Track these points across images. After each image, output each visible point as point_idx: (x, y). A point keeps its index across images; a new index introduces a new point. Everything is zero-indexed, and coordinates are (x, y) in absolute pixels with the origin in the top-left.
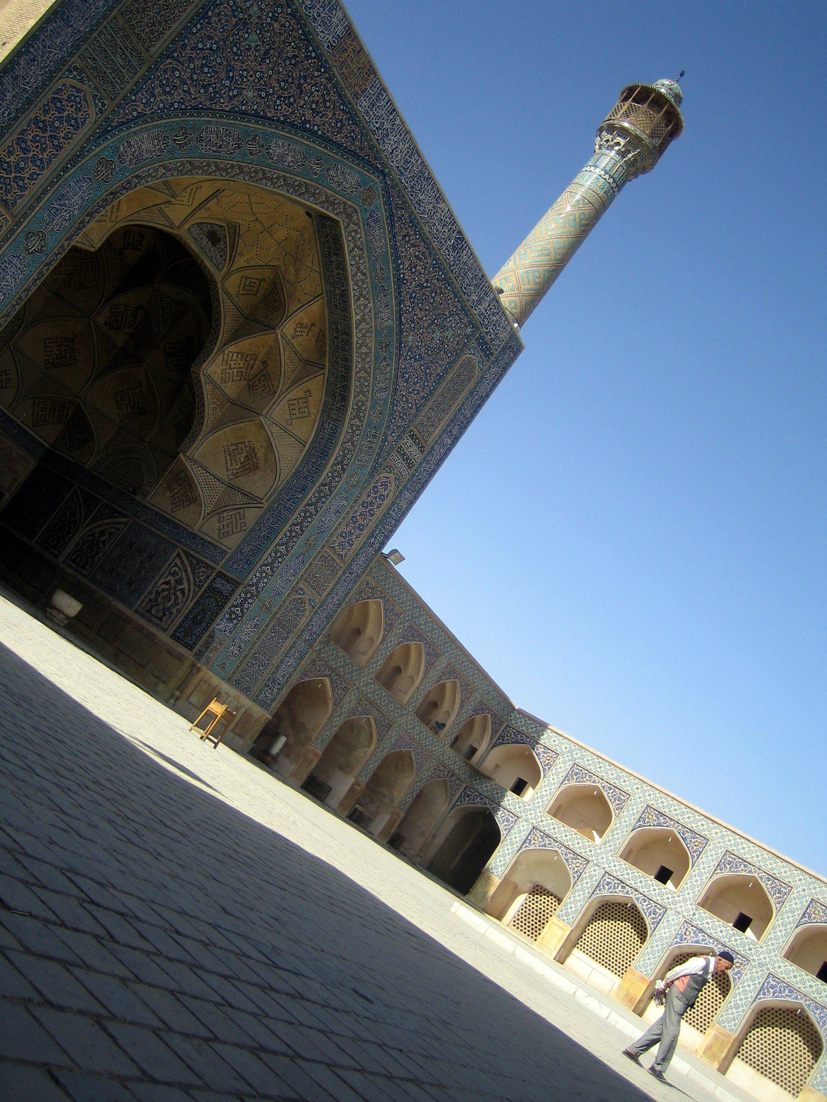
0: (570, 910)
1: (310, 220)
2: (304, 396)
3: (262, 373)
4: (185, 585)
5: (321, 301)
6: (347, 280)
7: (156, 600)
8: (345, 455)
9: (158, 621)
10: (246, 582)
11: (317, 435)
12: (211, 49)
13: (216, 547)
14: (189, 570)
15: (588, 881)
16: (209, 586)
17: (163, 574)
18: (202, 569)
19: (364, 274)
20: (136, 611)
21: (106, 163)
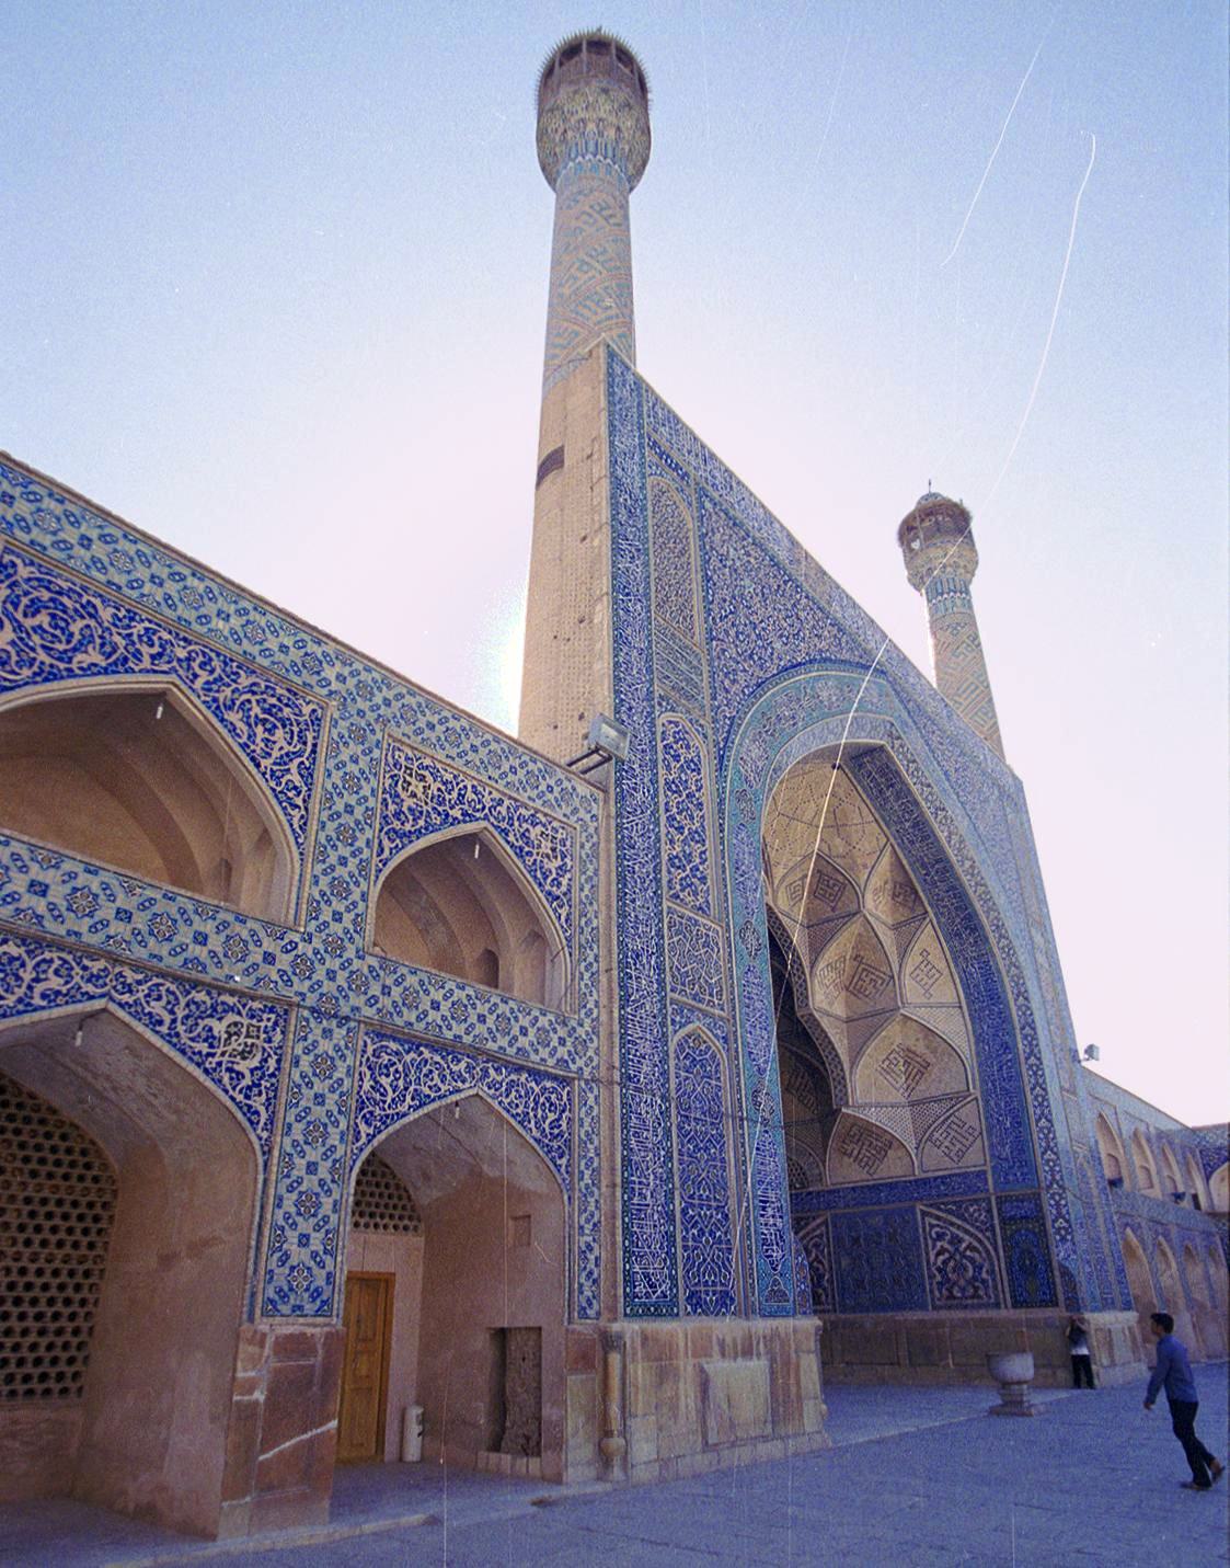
2: (921, 959)
4: (967, 1237)
5: (889, 848)
6: (916, 803)
7: (949, 1280)
8: (1017, 984)
9: (975, 1301)
10: (1043, 1185)
11: (966, 987)
12: (731, 612)
13: (965, 1175)
14: (954, 1220)
16: (1003, 1221)
19: (929, 786)
20: (935, 1308)
21: (741, 796)
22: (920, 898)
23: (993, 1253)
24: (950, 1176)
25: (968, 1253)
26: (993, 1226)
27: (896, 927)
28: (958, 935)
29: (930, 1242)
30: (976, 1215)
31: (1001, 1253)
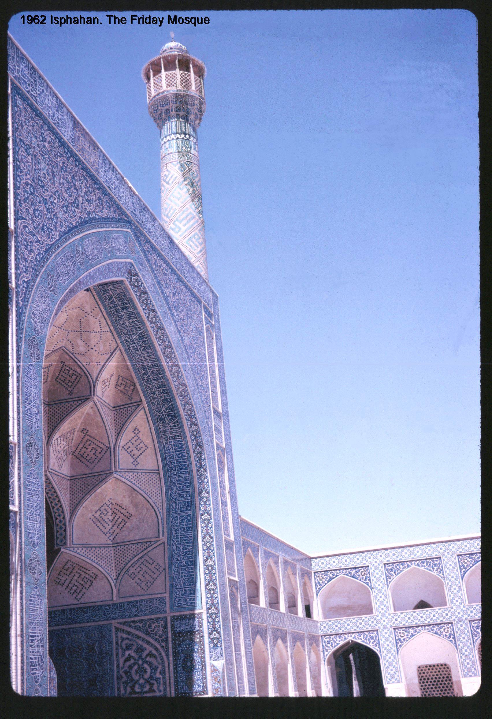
0: (469, 666)
1: (88, 293)
3: (85, 439)
4: (149, 648)
5: (118, 352)
6: (143, 324)
7: (132, 680)
11: (164, 459)
13: (151, 600)
15: (463, 636)
16: (174, 634)
17: (117, 654)
18: (153, 626)
22: (137, 391)
23: (165, 657)
24: (141, 601)
25: (148, 659)
26: (167, 638)
27: (116, 408)
28: (163, 420)
29: (120, 650)
30: (156, 630)
31: (171, 659)
